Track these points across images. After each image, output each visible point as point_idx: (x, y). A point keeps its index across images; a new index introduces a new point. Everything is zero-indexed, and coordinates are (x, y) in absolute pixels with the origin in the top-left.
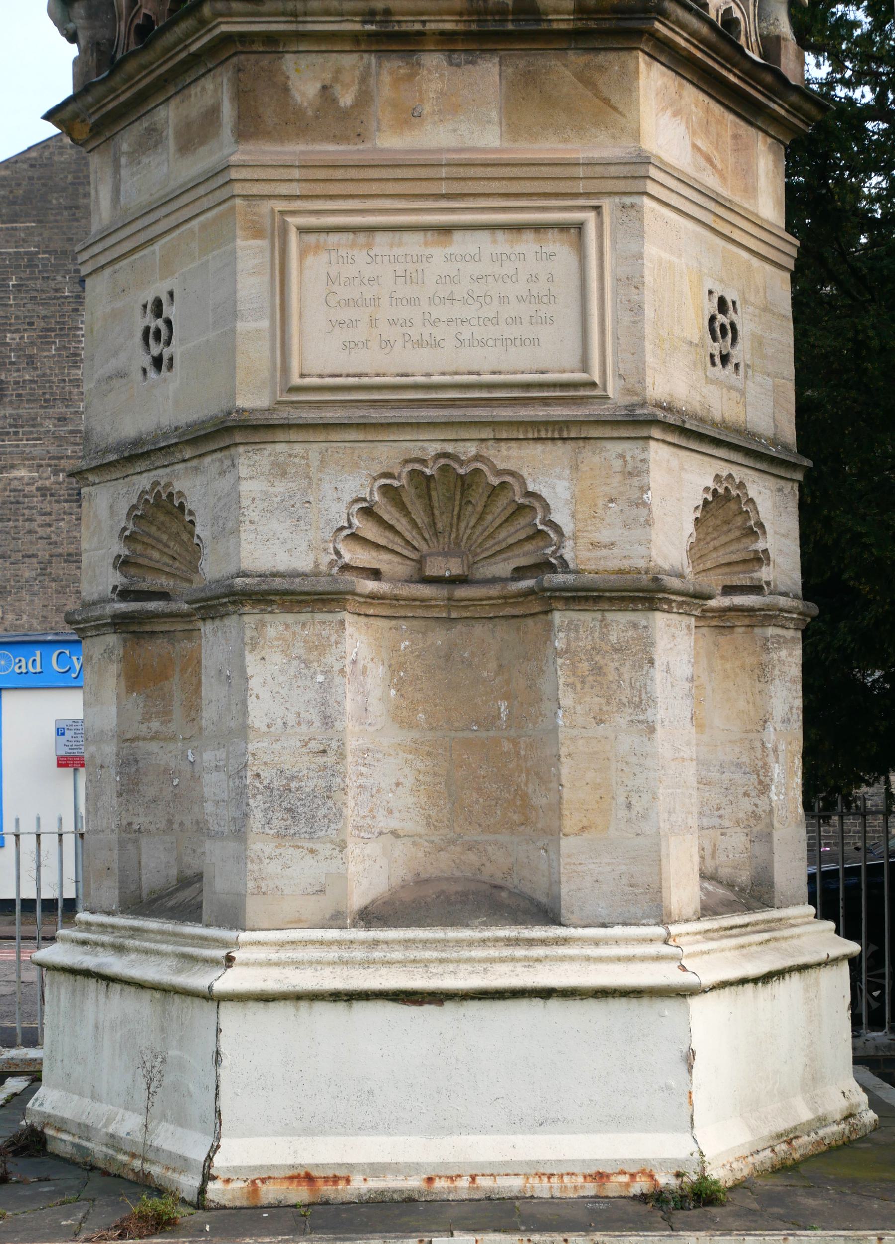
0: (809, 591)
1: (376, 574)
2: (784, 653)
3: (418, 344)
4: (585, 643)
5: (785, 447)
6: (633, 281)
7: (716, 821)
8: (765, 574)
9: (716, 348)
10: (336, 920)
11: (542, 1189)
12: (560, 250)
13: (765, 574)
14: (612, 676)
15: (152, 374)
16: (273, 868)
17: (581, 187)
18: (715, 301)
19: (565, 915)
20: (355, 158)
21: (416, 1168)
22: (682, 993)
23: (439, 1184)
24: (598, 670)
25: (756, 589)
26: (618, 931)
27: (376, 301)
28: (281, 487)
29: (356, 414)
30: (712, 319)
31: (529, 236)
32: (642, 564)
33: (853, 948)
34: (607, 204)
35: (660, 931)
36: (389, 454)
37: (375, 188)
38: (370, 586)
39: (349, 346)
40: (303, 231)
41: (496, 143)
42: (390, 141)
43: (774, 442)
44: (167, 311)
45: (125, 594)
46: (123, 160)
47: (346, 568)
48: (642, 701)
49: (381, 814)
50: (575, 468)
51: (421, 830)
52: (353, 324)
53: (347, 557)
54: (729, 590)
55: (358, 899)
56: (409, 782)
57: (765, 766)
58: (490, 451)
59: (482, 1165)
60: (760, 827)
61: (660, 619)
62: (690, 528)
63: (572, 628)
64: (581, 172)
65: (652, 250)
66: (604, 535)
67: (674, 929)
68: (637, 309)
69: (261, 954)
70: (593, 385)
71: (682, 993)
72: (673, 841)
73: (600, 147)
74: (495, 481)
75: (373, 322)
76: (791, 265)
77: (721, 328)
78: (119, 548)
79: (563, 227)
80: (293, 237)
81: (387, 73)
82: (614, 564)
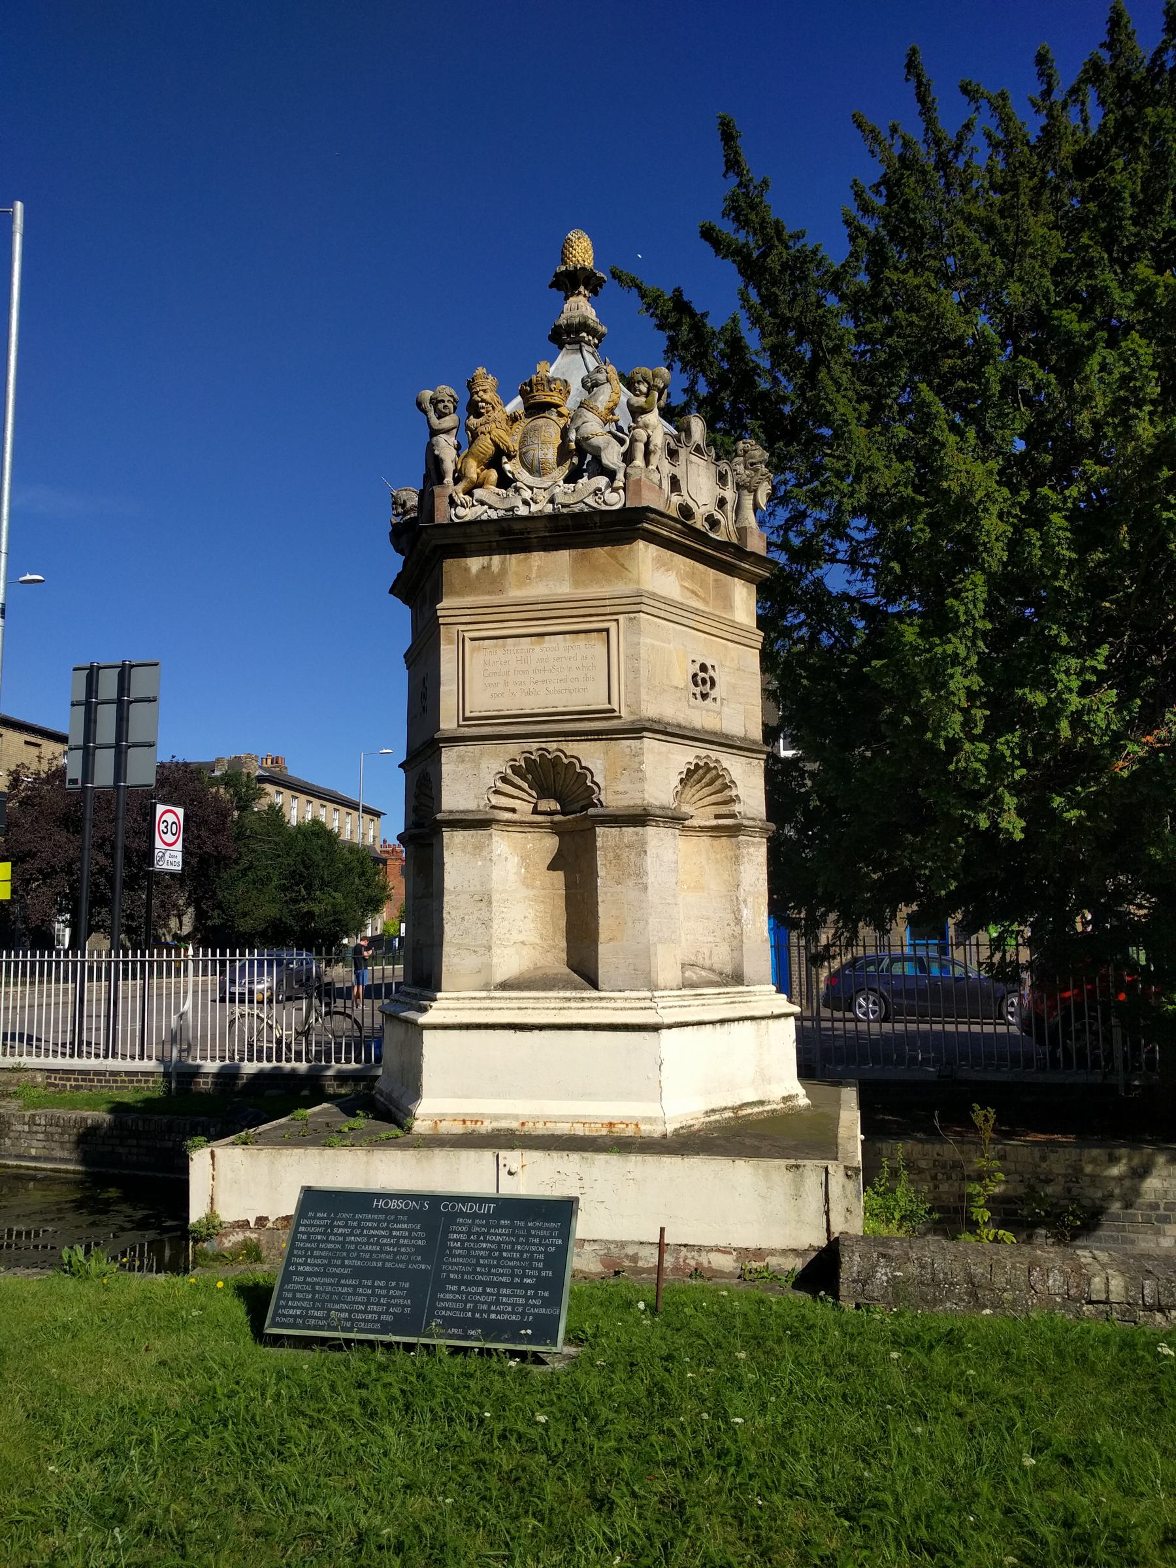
0: (770, 816)
1: (513, 810)
2: (752, 850)
3: (528, 694)
4: (611, 843)
5: (754, 742)
6: (634, 657)
7: (711, 939)
8: (736, 808)
9: (698, 690)
10: (486, 987)
11: (579, 1130)
12: (597, 642)
13: (736, 808)
14: (625, 860)
16: (456, 960)
17: (608, 610)
18: (697, 666)
19: (601, 985)
20: (496, 602)
21: (515, 1117)
22: (655, 1028)
23: (540, 1125)
24: (617, 857)
25: (733, 816)
26: (627, 994)
27: (507, 672)
28: (461, 767)
30: (695, 676)
31: (582, 635)
32: (639, 802)
33: (796, 1009)
34: (621, 617)
35: (649, 994)
37: (507, 616)
38: (508, 816)
40: (472, 639)
41: (567, 590)
42: (515, 593)
43: (744, 739)
47: (493, 807)
48: (640, 873)
49: (515, 932)
50: (606, 753)
51: (538, 941)
52: (496, 685)
53: (494, 802)
54: (717, 817)
55: (499, 978)
56: (531, 916)
57: (739, 910)
59: (549, 1116)
60: (735, 943)
61: (650, 830)
62: (675, 781)
63: (605, 835)
64: (608, 602)
65: (645, 640)
66: (621, 788)
67: (656, 994)
68: (636, 671)
70: (613, 711)
71: (655, 1028)
72: (659, 947)
73: (620, 588)
74: (566, 761)
75: (506, 683)
76: (759, 646)
77: (703, 680)
80: (467, 641)
81: (514, 560)
82: (625, 803)
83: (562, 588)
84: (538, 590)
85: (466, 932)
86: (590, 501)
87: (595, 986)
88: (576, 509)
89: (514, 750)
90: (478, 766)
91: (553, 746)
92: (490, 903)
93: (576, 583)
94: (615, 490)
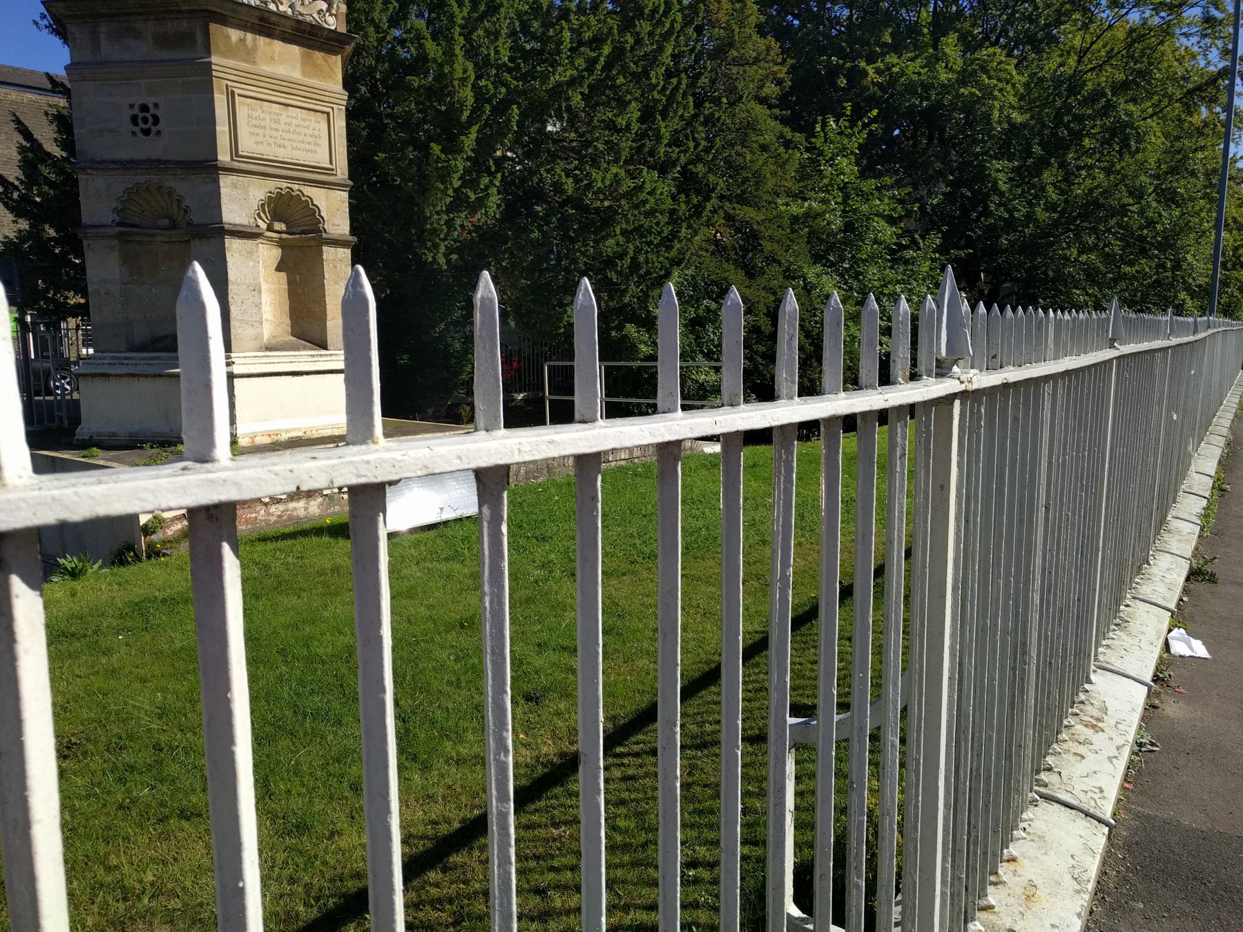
10: (260, 350)
15: (140, 135)
17: (327, 99)
21: (299, 429)
24: (335, 267)
29: (262, 169)
36: (272, 185)
39: (256, 143)
42: (265, 68)
44: (152, 110)
45: (119, 224)
46: (102, 36)
58: (302, 188)
66: (336, 222)
69: (243, 361)
78: (115, 204)
79: (323, 112)
81: (262, 41)
83: (297, 75)
84: (281, 70)
85: (245, 312)
86: (315, 15)
87: (325, 348)
88: (308, 19)
89: (272, 185)
90: (247, 193)
91: (295, 187)
92: (260, 292)
93: (304, 74)
94: (331, 15)
